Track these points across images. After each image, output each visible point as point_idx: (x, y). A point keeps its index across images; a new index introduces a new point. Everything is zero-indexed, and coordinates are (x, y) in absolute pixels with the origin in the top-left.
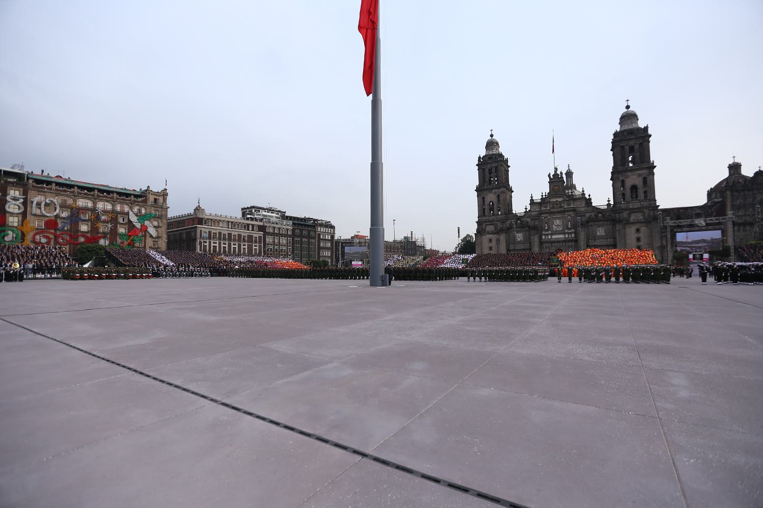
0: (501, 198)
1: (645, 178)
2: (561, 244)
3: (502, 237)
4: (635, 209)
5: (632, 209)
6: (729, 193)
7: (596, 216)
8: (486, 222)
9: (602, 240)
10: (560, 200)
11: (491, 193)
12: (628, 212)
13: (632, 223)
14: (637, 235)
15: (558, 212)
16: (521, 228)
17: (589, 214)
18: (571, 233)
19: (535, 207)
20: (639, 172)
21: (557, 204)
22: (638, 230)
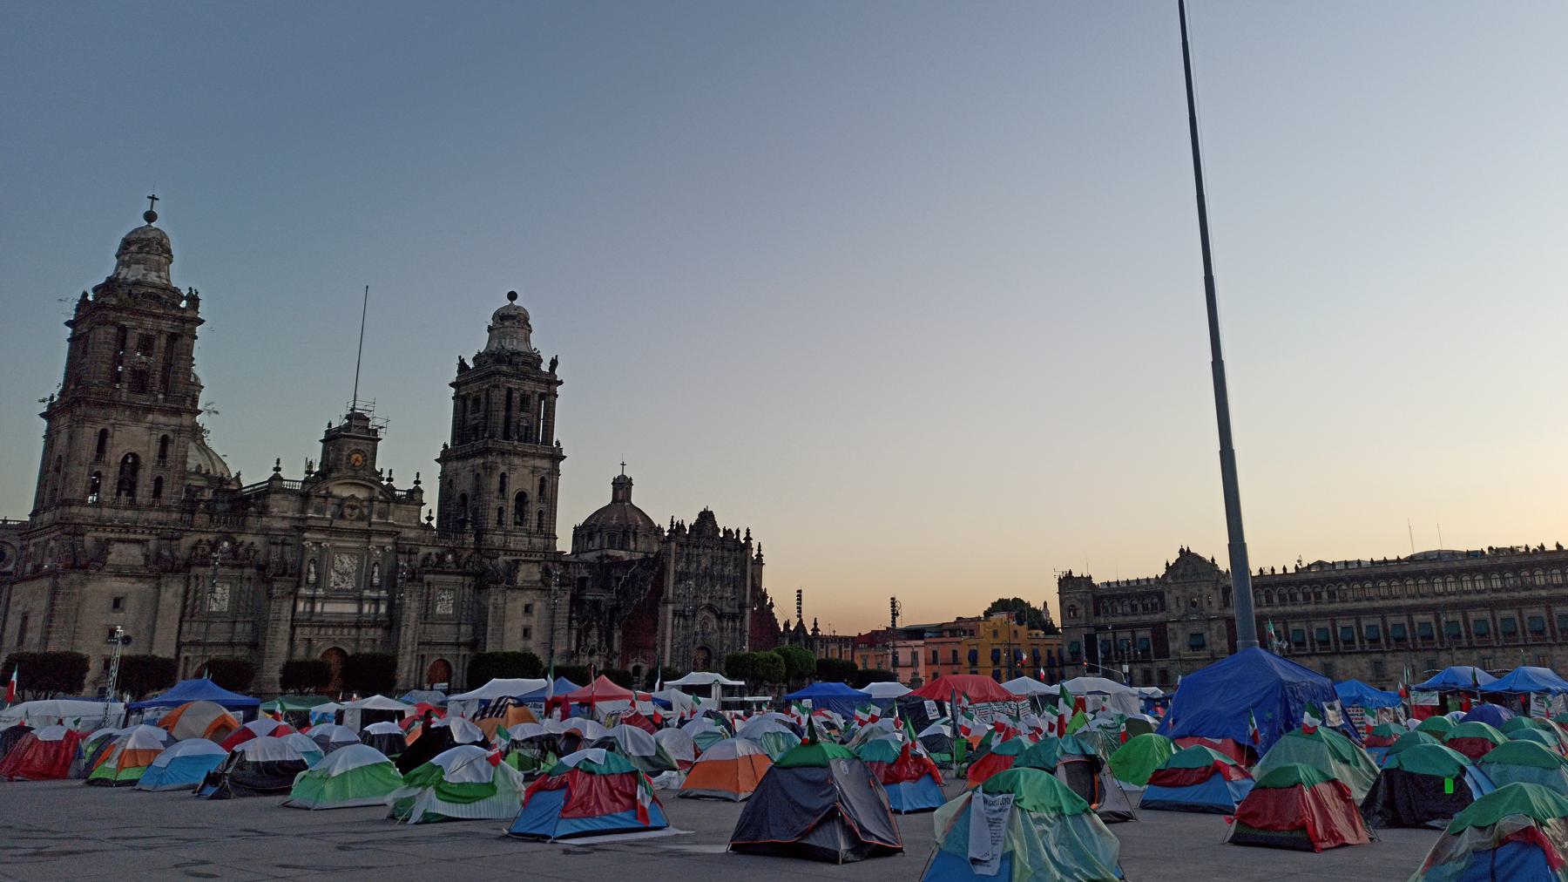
0: (171, 449)
1: (542, 479)
2: (346, 631)
3: (172, 593)
7: (441, 557)
8: (99, 524)
9: (445, 628)
10: (361, 494)
11: (137, 421)
13: (521, 589)
15: (352, 532)
16: (233, 567)
18: (376, 601)
19: (285, 503)
20: (538, 463)
21: (353, 508)
22: (528, 609)
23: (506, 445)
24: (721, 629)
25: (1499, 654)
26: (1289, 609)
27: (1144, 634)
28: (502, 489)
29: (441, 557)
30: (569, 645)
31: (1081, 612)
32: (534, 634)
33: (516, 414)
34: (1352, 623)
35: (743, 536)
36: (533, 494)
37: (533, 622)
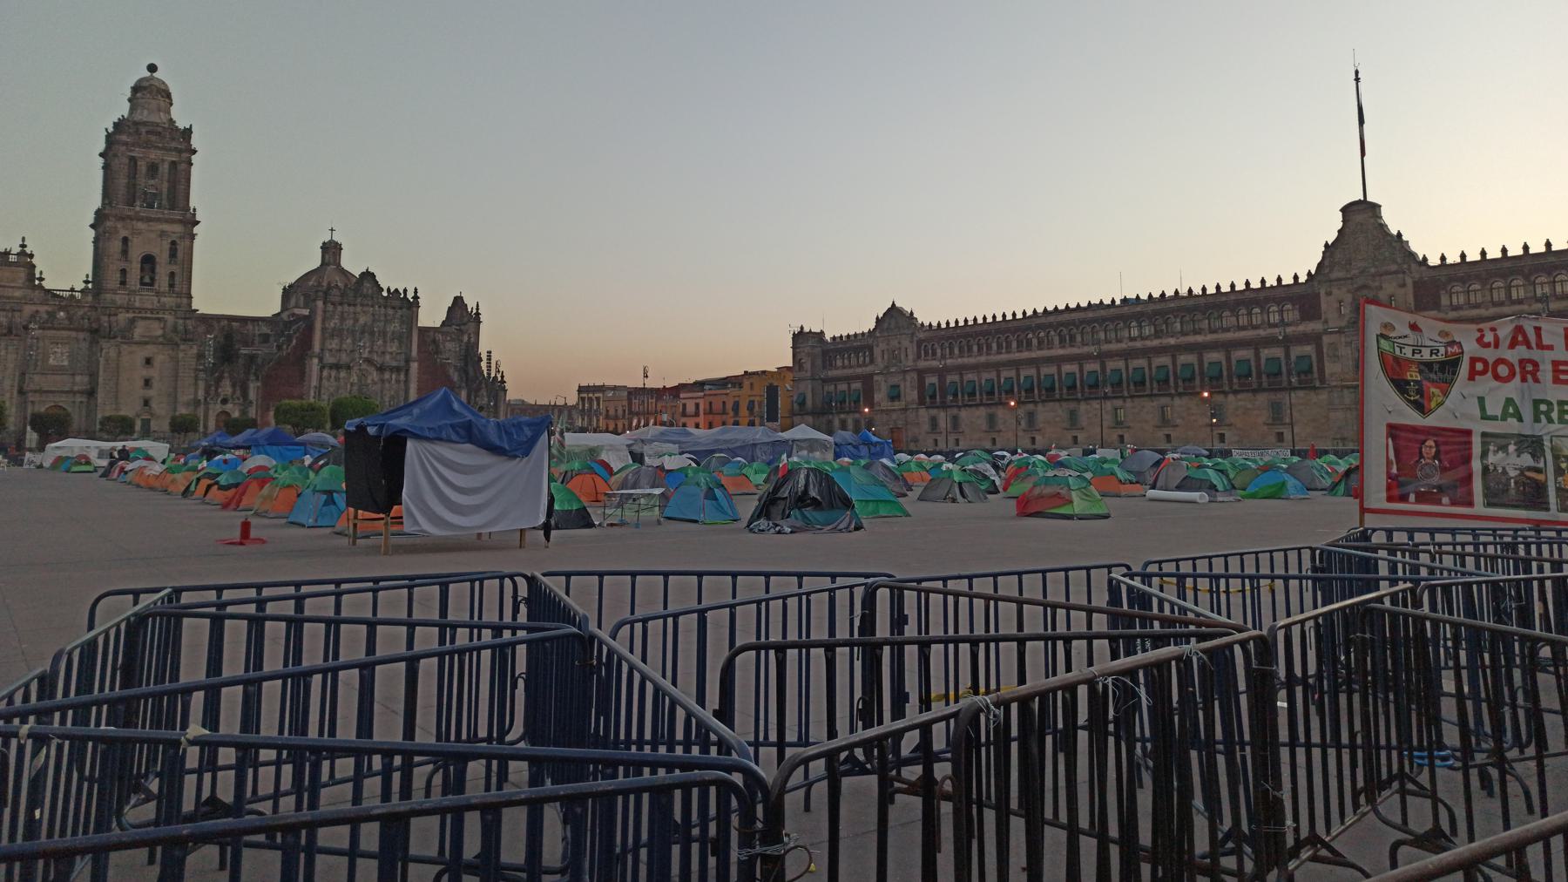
4: (146, 310)
5: (141, 310)
6: (320, 304)
7: (52, 315)
12: (131, 315)
14: (145, 373)
17: (34, 308)
22: (148, 361)
23: (128, 211)
24: (383, 381)
25: (1129, 403)
26: (966, 360)
27: (857, 385)
28: (125, 252)
29: (52, 315)
30: (196, 392)
31: (808, 366)
32: (156, 384)
33: (142, 181)
34: (1012, 373)
35: (410, 296)
36: (162, 256)
37: (153, 372)
